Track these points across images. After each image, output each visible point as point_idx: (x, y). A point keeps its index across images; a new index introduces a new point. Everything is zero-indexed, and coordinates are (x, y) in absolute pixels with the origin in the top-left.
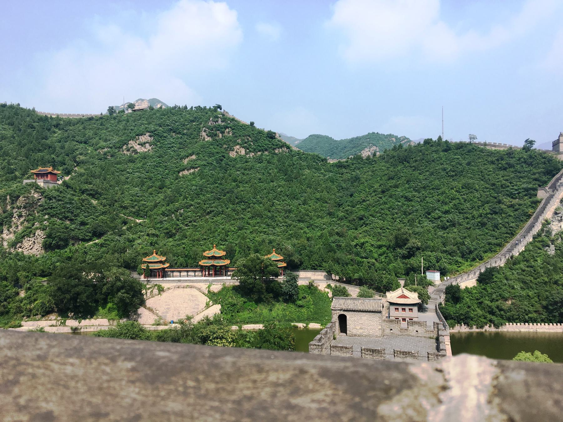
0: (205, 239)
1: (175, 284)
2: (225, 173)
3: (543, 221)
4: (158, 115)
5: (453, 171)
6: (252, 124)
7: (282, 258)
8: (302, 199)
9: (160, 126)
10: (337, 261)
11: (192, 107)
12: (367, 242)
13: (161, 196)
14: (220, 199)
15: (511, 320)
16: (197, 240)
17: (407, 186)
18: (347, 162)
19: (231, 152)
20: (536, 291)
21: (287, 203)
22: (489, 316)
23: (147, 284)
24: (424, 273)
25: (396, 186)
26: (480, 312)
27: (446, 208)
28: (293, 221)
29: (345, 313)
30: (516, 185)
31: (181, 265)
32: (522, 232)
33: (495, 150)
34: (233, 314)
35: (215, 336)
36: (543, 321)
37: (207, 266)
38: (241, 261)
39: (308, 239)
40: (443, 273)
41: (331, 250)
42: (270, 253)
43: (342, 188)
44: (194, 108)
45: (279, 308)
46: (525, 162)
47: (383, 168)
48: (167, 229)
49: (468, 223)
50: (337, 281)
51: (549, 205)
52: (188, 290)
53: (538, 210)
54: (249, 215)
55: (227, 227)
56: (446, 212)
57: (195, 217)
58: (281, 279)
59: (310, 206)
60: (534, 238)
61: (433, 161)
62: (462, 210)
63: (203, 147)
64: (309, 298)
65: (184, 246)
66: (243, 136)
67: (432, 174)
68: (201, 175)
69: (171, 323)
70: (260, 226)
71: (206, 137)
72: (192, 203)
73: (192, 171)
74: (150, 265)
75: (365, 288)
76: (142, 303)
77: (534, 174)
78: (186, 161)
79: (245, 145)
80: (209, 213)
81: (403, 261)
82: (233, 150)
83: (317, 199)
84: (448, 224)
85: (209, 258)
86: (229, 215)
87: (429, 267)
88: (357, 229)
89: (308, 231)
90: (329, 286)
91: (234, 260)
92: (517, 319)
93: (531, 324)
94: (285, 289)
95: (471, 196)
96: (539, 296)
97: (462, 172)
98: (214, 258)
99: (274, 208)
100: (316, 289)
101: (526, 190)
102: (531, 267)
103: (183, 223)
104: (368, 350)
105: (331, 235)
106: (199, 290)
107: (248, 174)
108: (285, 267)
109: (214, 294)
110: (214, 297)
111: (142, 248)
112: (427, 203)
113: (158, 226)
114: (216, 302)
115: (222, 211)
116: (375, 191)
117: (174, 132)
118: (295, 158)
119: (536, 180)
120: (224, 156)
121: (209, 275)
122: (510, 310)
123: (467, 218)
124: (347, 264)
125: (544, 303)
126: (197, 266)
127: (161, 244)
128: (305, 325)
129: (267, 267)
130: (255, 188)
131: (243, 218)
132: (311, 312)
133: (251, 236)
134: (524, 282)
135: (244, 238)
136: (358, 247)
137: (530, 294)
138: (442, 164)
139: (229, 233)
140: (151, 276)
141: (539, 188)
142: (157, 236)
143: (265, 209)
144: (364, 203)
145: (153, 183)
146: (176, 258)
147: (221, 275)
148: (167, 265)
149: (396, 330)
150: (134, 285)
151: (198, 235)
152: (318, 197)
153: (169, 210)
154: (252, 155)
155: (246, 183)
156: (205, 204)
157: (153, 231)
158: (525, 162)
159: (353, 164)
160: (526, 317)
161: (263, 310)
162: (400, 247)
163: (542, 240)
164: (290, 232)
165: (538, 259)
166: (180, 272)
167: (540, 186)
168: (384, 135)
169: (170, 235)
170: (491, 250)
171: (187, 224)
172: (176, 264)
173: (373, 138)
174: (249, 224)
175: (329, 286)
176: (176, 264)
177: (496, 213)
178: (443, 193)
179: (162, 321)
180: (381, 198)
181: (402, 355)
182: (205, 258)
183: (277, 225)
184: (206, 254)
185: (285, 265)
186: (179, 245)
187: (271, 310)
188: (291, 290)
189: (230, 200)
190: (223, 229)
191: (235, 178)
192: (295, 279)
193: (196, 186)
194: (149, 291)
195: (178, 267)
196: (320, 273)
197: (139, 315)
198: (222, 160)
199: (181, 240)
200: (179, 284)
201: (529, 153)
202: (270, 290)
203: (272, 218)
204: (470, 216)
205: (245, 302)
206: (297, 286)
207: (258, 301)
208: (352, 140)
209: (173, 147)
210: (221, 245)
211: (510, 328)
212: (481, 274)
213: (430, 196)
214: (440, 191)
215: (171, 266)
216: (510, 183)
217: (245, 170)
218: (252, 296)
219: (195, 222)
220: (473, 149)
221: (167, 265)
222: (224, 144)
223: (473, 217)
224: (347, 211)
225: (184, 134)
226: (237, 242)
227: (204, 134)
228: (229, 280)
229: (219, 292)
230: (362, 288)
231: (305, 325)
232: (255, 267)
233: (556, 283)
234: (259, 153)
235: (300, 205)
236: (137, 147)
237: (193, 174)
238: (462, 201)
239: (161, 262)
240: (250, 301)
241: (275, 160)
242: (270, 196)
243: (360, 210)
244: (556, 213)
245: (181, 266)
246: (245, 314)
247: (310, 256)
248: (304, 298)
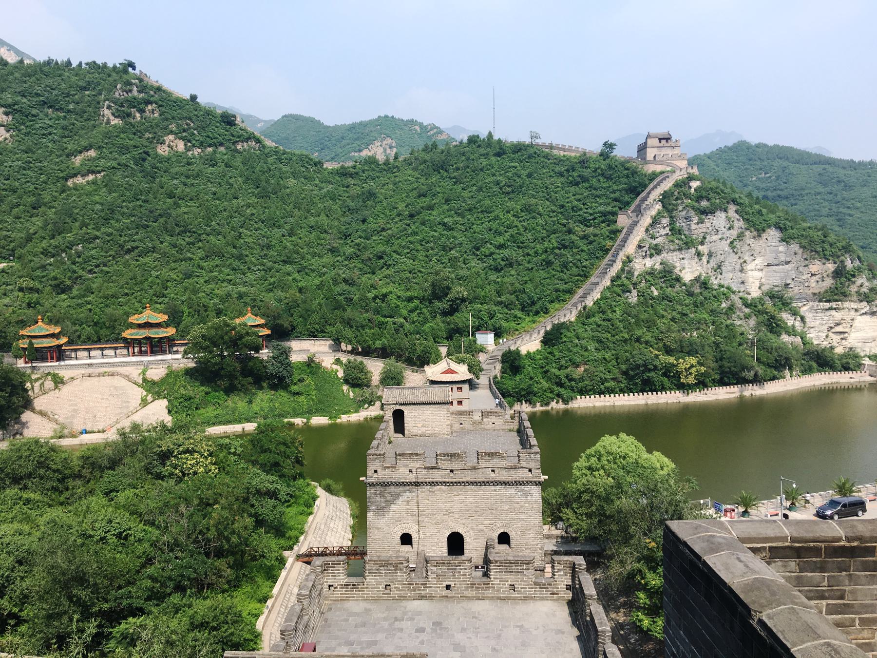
0: (127, 294)
1: (83, 371)
2: (153, 182)
3: (624, 258)
4: (17, 75)
5: (509, 186)
6: (194, 98)
7: (263, 321)
8: (287, 226)
9: (24, 96)
10: (348, 323)
11: (80, 63)
12: (391, 292)
13: (38, 222)
14: (148, 226)
15: (583, 392)
16: (113, 296)
17: (446, 207)
18: (354, 167)
19: (159, 146)
20: (614, 352)
21: (263, 233)
22: (557, 389)
23: (33, 373)
24: (473, 334)
25: (430, 208)
26: (545, 385)
27: (500, 240)
28: (275, 262)
29: (402, 408)
30: (591, 208)
31: (89, 339)
32: (596, 273)
33: (564, 156)
34: (190, 412)
35: (181, 449)
36: (622, 391)
37: (136, 339)
38: (198, 330)
39: (300, 290)
40: (498, 334)
41: (338, 307)
42: (241, 314)
43: (349, 210)
44: (84, 66)
45: (264, 398)
46: (603, 174)
47: (410, 178)
48: (55, 278)
49: (529, 262)
50: (349, 352)
51: (632, 236)
52: (108, 379)
53: (618, 242)
54: (201, 253)
55: (165, 273)
56: (501, 246)
57: (106, 257)
58: (265, 354)
59: (300, 238)
60: (612, 281)
61: (482, 170)
62: (522, 243)
63: (107, 135)
64: (309, 380)
65: (89, 306)
66: (180, 119)
67: (480, 189)
68: (108, 184)
69: (82, 433)
70: (220, 272)
71: (112, 118)
72: (98, 233)
73: (91, 177)
74: (34, 341)
75: (392, 361)
76: (28, 404)
77: (614, 192)
78: (78, 160)
79: (184, 134)
80: (129, 251)
81: (444, 319)
82: (163, 143)
83: (312, 227)
84: (503, 263)
85: (140, 326)
86: (165, 253)
87: (479, 326)
88: (374, 273)
89: (299, 278)
90: (338, 361)
91: (182, 326)
92: (590, 390)
93: (607, 396)
94: (271, 369)
95: (532, 223)
96: (617, 359)
97: (521, 187)
98: (148, 325)
99: (242, 241)
100: (319, 366)
101: (604, 214)
102: (609, 320)
103: (83, 269)
104: (445, 455)
105: (336, 282)
106: (127, 378)
107: (192, 185)
108: (268, 336)
109: (154, 383)
110: (154, 389)
111: (14, 312)
112: (475, 232)
113: (39, 273)
114: (158, 396)
115: (154, 248)
116: (399, 215)
117: (51, 107)
118: (270, 160)
119: (616, 200)
120: (147, 153)
121: (141, 353)
122: (582, 379)
123: (528, 255)
124: (363, 327)
125: (624, 367)
126: (116, 340)
127: (47, 305)
128: (305, 420)
129: (241, 337)
130: (208, 209)
131: (191, 259)
132: (313, 400)
133: (207, 288)
134: (600, 341)
135: (195, 292)
136: (378, 300)
137: (607, 356)
138: (494, 175)
139: (169, 284)
140: (36, 360)
141: (620, 212)
142: (38, 291)
143: (228, 244)
144: (384, 233)
145: (20, 198)
146: (78, 327)
147: (163, 352)
148: (64, 340)
149: (467, 425)
150: (11, 375)
151: (112, 289)
152: (313, 224)
153: (56, 247)
154: (197, 151)
155: (191, 200)
156: (121, 236)
157: (31, 284)
158: (603, 174)
159: (363, 172)
160: (602, 387)
161: (238, 402)
162: (439, 299)
163: (620, 285)
164: (272, 280)
165: (617, 309)
166: (89, 350)
167: (620, 209)
168: (403, 120)
169: (61, 289)
170: (558, 300)
171: (91, 270)
172: (79, 337)
173: (386, 126)
174: (202, 269)
175: (338, 361)
176: (79, 337)
177: (565, 247)
178: (496, 218)
179: (66, 432)
180: (409, 225)
181: (487, 458)
182: (131, 326)
183: (249, 268)
184: (133, 319)
185: (269, 332)
186: (80, 306)
187: (250, 402)
188: (281, 370)
189: (166, 229)
190: (157, 277)
191: (171, 191)
192: (286, 352)
193: (102, 204)
194: (37, 385)
195: (84, 343)
196: (322, 342)
197: (24, 425)
198: (144, 160)
199: (84, 296)
200: (90, 370)
201: (607, 161)
202: (247, 372)
203: (240, 257)
204: (531, 252)
205: (207, 394)
206: (289, 364)
207: (230, 390)
208: (353, 127)
209: (50, 134)
210: (156, 303)
211: (583, 403)
212: (547, 333)
213: (479, 222)
214: (492, 215)
215: (70, 342)
216: (584, 204)
217: (188, 177)
218: (218, 383)
219: (105, 265)
220: (535, 153)
221: (64, 340)
222: (146, 131)
223: (536, 252)
224: (358, 245)
225: (69, 111)
226: (183, 298)
227: (107, 112)
228: (178, 360)
229: (163, 381)
230: (387, 360)
231: (305, 420)
232: (222, 338)
233: (638, 340)
234: (210, 149)
235: (283, 236)
237: (94, 182)
238: (522, 230)
239: (53, 336)
240: (216, 391)
241: (238, 162)
242: (235, 222)
243: (378, 244)
244: (640, 247)
245: (89, 340)
246: (209, 412)
247: (306, 317)
248: (301, 380)
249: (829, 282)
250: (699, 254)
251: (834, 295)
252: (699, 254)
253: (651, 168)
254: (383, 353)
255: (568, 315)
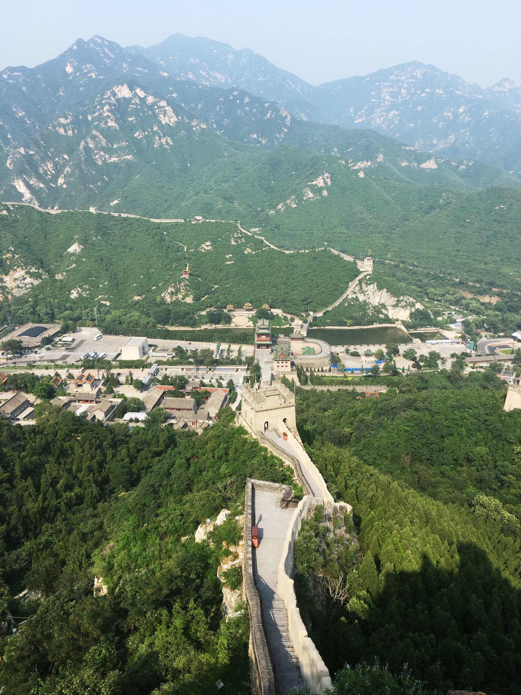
40: (314, 312)
114: (251, 320)
154: (254, 252)
211: (327, 327)
236: (205, 247)
249: (395, 303)
250: (365, 295)
251: (395, 306)
252: (365, 295)
253: (361, 270)
254: (291, 314)
255: (330, 309)
